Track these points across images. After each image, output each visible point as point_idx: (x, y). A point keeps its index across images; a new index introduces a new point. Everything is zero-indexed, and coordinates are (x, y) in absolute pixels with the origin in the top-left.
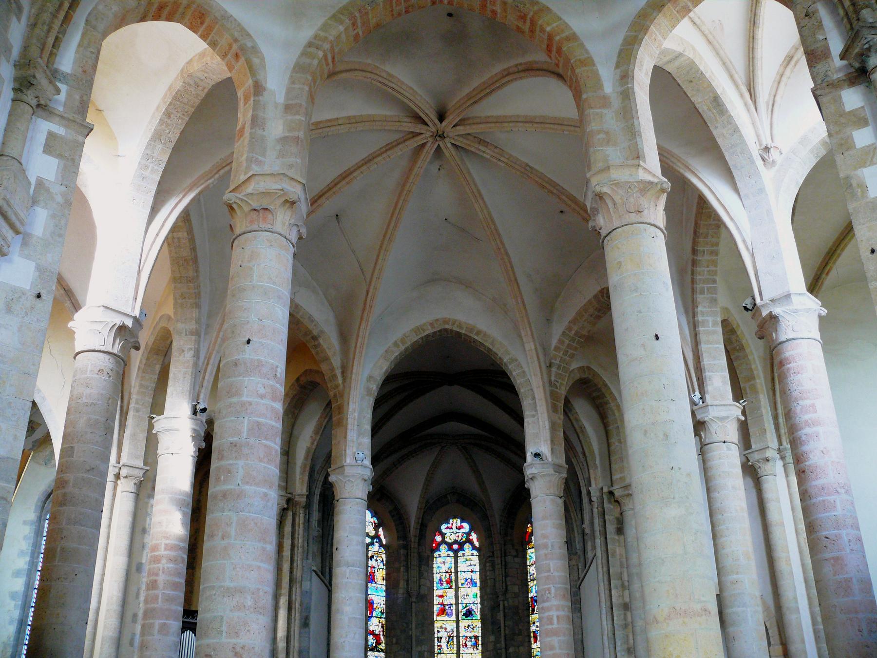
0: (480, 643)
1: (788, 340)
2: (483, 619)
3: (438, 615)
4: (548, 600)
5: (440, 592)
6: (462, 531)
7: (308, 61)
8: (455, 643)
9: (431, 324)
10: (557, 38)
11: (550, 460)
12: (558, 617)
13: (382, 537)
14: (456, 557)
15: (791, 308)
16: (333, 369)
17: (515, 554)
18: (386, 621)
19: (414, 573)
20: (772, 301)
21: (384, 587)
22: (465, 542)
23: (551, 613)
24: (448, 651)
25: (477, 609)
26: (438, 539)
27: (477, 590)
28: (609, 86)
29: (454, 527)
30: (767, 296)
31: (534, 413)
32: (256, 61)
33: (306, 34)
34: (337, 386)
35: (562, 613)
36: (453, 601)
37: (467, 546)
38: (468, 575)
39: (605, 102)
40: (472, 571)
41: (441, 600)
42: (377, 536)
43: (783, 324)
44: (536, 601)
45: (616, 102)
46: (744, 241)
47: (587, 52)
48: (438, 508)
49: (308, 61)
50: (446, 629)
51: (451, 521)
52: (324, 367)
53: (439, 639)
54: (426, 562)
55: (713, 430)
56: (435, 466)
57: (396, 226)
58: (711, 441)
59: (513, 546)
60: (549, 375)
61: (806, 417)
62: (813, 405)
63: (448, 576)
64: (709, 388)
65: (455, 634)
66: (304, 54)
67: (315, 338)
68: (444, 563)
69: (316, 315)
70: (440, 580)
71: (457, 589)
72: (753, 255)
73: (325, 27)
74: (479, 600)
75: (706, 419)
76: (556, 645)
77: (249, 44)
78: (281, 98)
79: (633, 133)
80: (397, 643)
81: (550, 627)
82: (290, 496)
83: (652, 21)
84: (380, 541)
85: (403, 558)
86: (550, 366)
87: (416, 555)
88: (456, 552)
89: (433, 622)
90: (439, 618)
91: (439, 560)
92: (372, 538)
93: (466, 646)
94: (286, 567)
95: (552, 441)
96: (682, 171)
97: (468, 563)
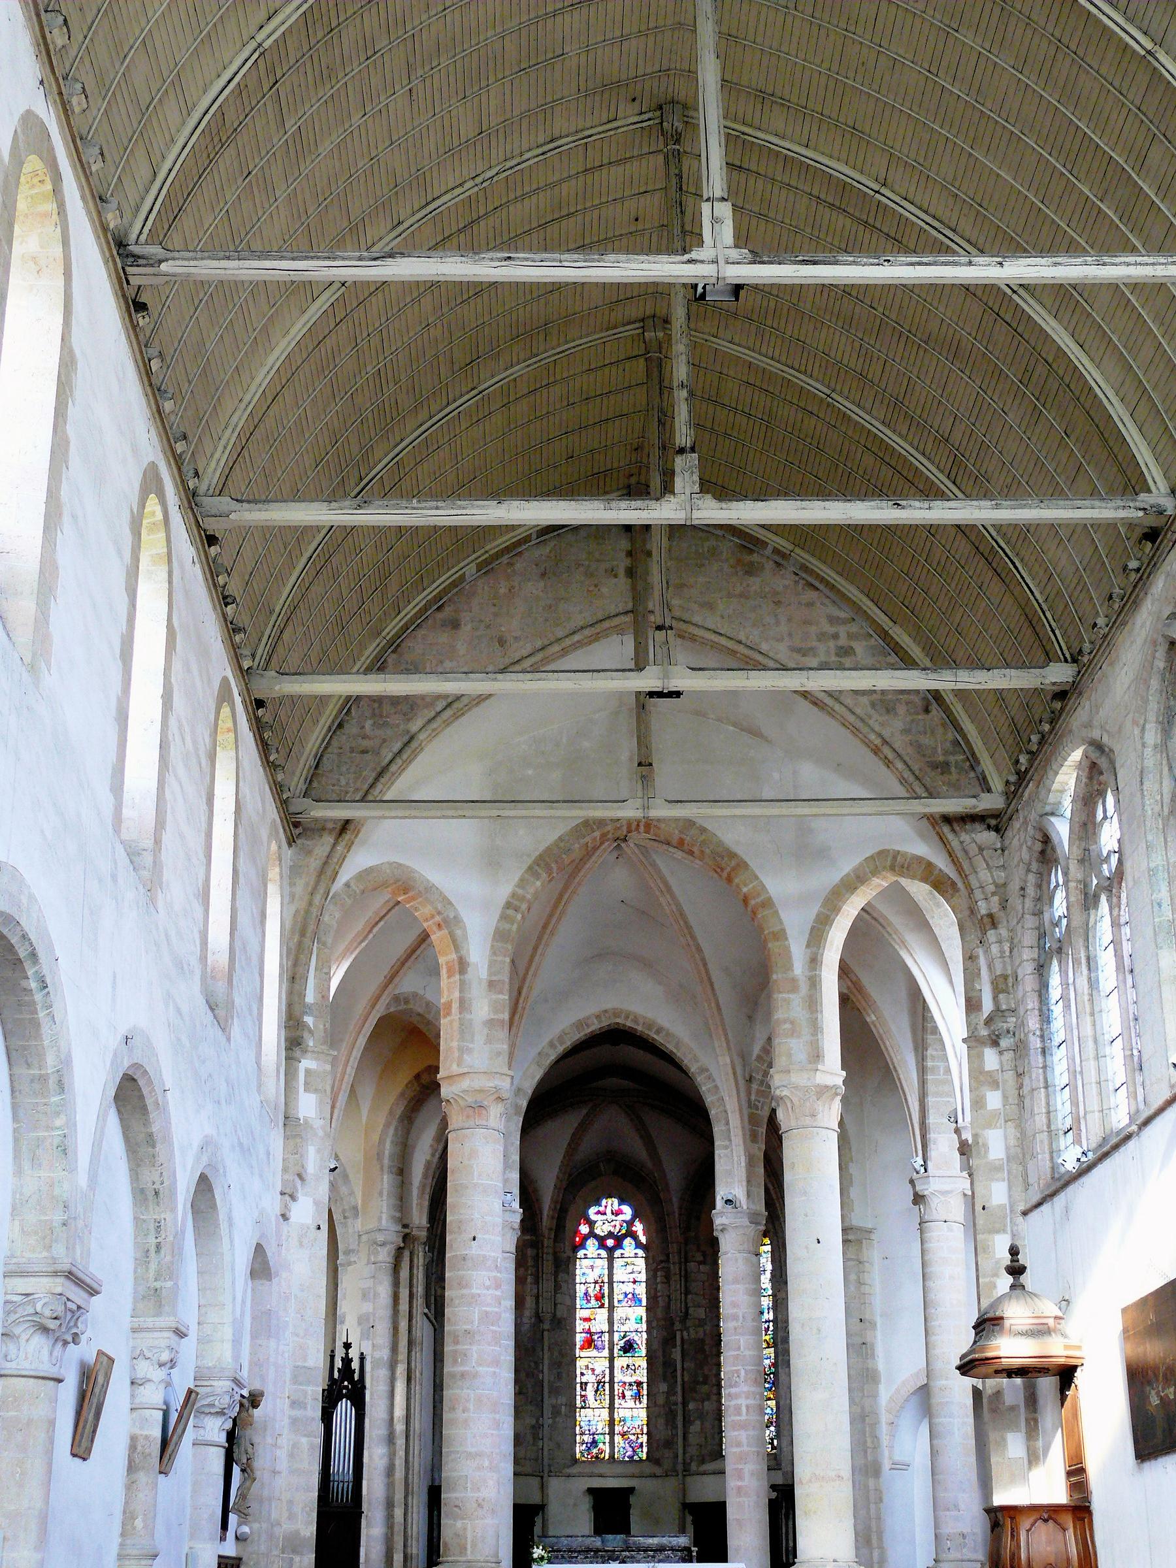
0: (645, 1392)
3: (582, 1348)
4: (736, 1385)
6: (621, 1217)
7: (507, 926)
8: (607, 1392)
9: (598, 1017)
11: (745, 1207)
12: (747, 1407)
17: (701, 1258)
22: (625, 1236)
23: (739, 1401)
24: (596, 1405)
25: (641, 1340)
26: (584, 1229)
27: (641, 1311)
28: (799, 968)
29: (608, 1211)
31: (727, 1143)
32: (458, 932)
33: (504, 891)
35: (751, 1402)
36: (606, 1328)
37: (628, 1242)
38: (629, 1288)
40: (635, 1282)
41: (586, 1325)
47: (781, 923)
48: (585, 1181)
49: (507, 926)
50: (593, 1370)
51: (604, 1202)
53: (584, 1385)
54: (564, 1266)
55: (933, 1206)
56: (582, 1128)
57: (559, 919)
58: (930, 1218)
60: (749, 1093)
63: (598, 1288)
65: (607, 1379)
66: (504, 917)
68: (592, 1267)
71: (611, 1309)
73: (522, 883)
76: (744, 1441)
77: (452, 915)
78: (484, 973)
79: (816, 1027)
82: (407, 1231)
85: (530, 1263)
86: (750, 1080)
87: (550, 1257)
88: (611, 1251)
89: (574, 1360)
91: (585, 1262)
93: (624, 1397)
94: (403, 1325)
95: (748, 1182)
96: (897, 947)
97: (629, 1268)
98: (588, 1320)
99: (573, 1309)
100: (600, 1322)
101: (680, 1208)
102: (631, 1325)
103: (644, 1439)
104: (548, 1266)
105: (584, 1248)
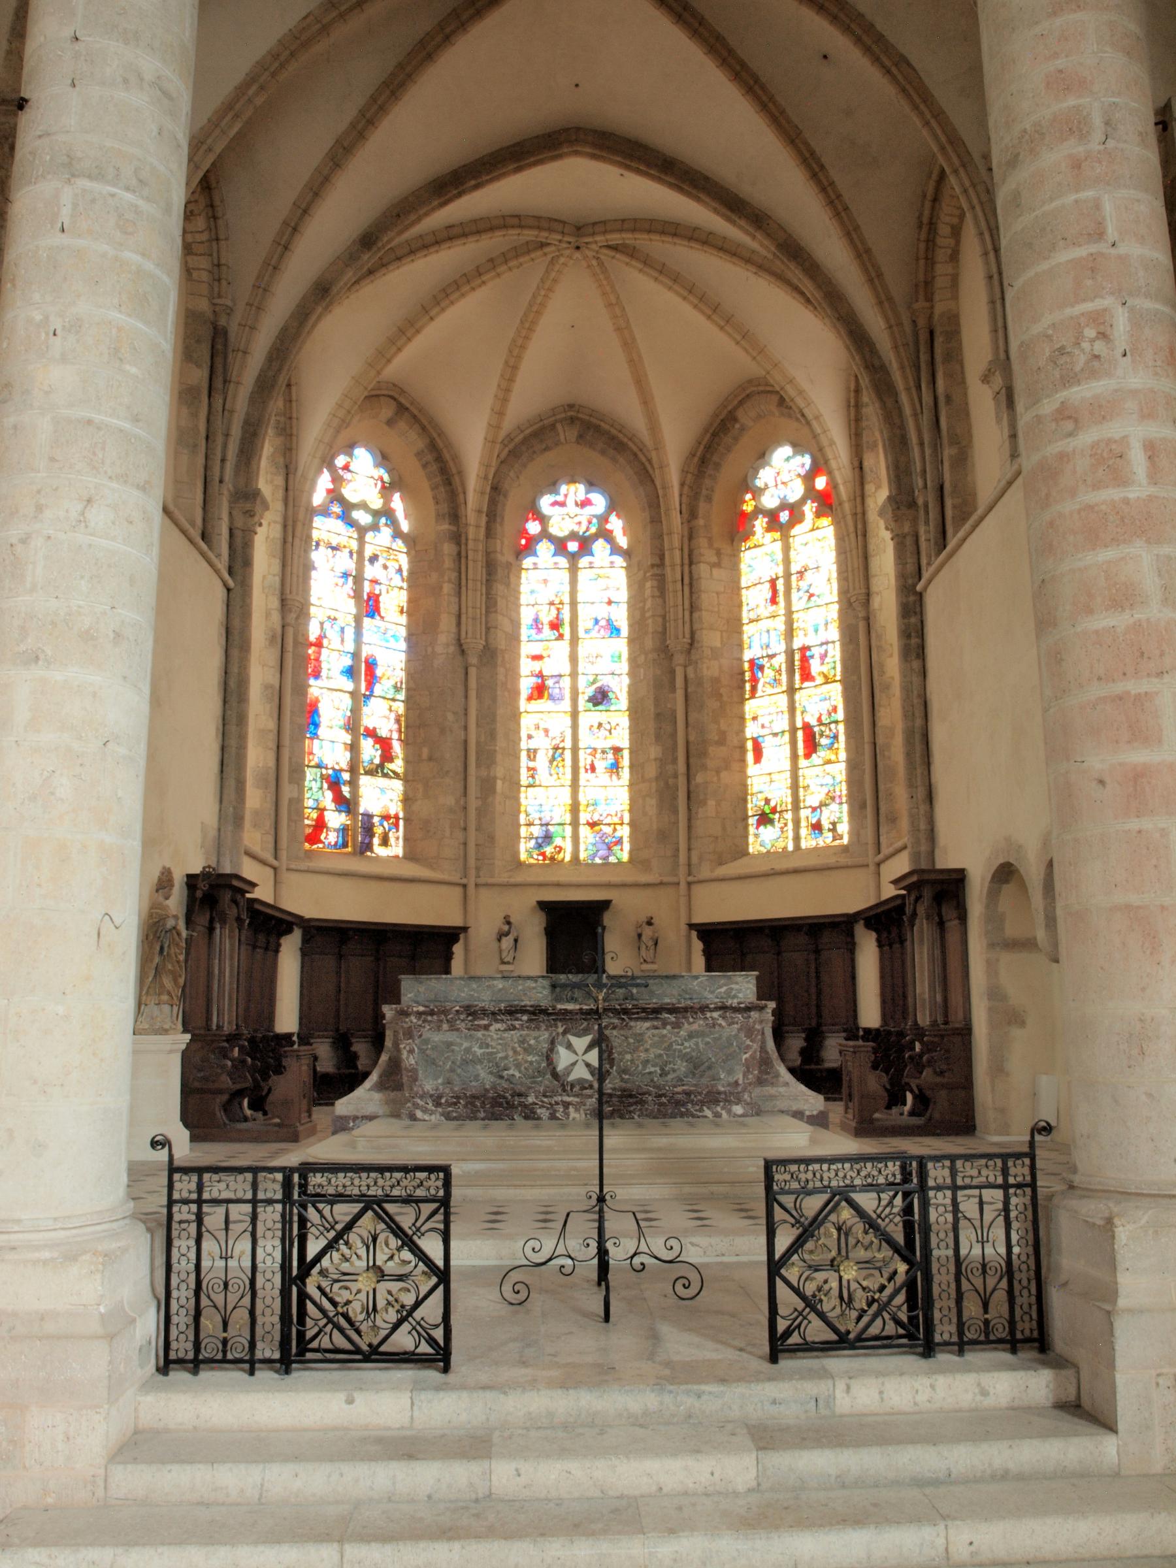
0: (626, 762)
2: (635, 711)
3: (530, 698)
5: (536, 649)
6: (589, 510)
13: (400, 513)
14: (573, 570)
17: (714, 559)
18: (407, 709)
19: (474, 598)
21: (403, 632)
22: (596, 537)
23: (1114, 430)
24: (551, 781)
25: (620, 687)
27: (621, 646)
29: (570, 502)
36: (566, 669)
37: (600, 546)
38: (602, 612)
40: (610, 603)
41: (536, 666)
42: (387, 512)
44: (761, 668)
50: (546, 731)
51: (564, 489)
53: (532, 754)
59: (710, 539)
63: (554, 613)
65: (568, 744)
68: (545, 581)
70: (536, 620)
80: (430, 759)
81: (1112, 494)
84: (394, 523)
85: (448, 563)
87: (480, 556)
88: (573, 558)
89: (515, 716)
92: (376, 514)
93: (593, 768)
97: (602, 583)
98: (538, 658)
99: (515, 638)
100: (557, 661)
101: (682, 485)
102: (603, 666)
103: (625, 832)
104: (476, 570)
105: (535, 554)
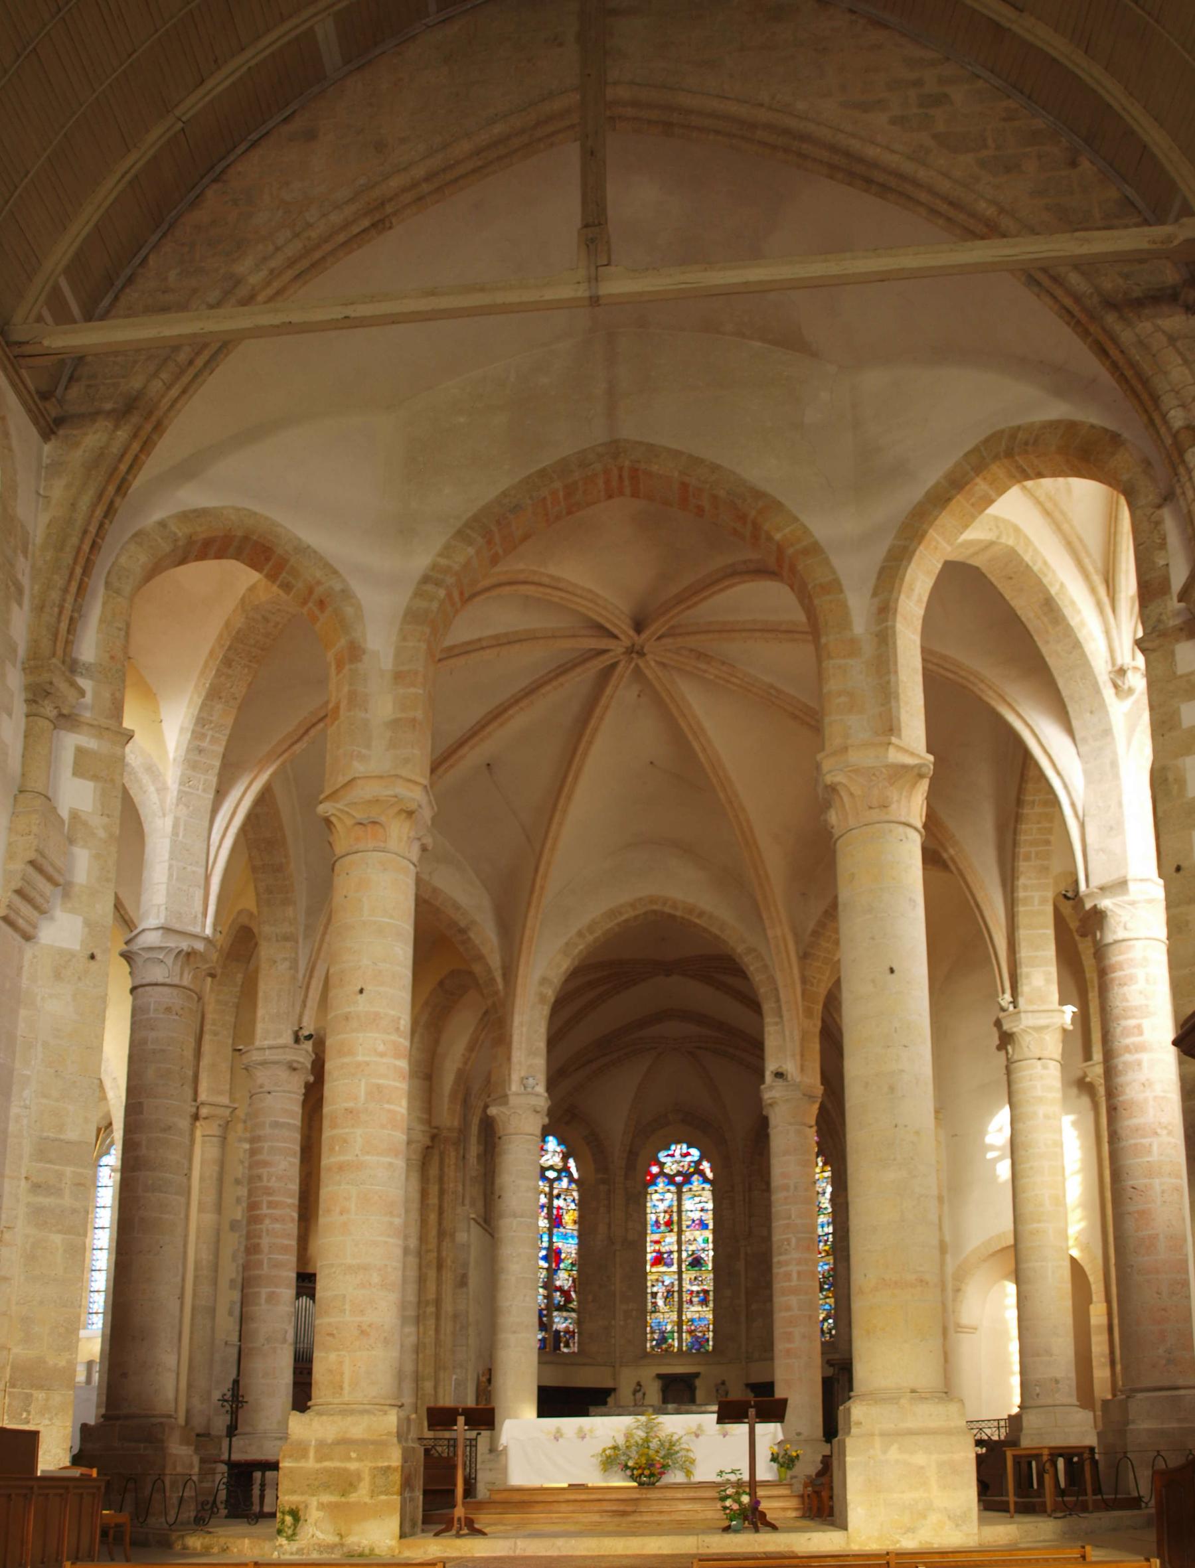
0: (711, 1298)
1: (1124, 940)
5: (656, 1237)
10: (790, 551)
13: (573, 1170)
15: (1126, 898)
16: (489, 971)
20: (1102, 889)
21: (576, 1233)
25: (708, 1256)
27: (709, 1234)
30: (1095, 882)
34: (496, 993)
36: (675, 1248)
38: (696, 1215)
39: (853, 647)
41: (657, 1247)
42: (566, 1169)
43: (1112, 921)
45: (868, 649)
46: (1073, 805)
52: (477, 968)
61: (1128, 1041)
62: (1139, 1027)
64: (1025, 989)
67: (463, 931)
68: (662, 1200)
69: (463, 899)
70: (657, 1222)
71: (680, 1233)
72: (1082, 826)
74: (711, 1246)
75: (1015, 1030)
83: (931, 524)
84: (570, 1175)
89: (645, 1274)
90: (654, 1270)
92: (559, 1171)
98: (657, 1242)
105: (655, 1184)
